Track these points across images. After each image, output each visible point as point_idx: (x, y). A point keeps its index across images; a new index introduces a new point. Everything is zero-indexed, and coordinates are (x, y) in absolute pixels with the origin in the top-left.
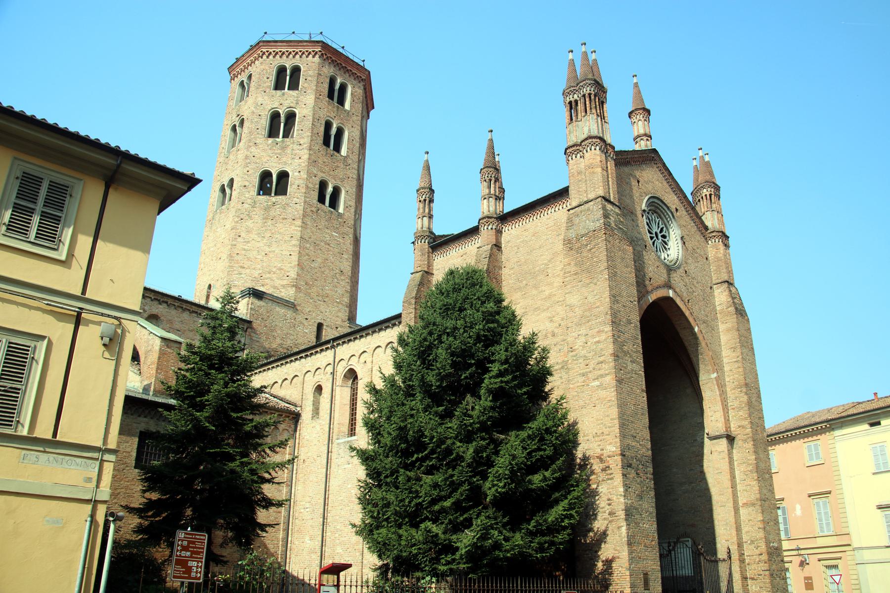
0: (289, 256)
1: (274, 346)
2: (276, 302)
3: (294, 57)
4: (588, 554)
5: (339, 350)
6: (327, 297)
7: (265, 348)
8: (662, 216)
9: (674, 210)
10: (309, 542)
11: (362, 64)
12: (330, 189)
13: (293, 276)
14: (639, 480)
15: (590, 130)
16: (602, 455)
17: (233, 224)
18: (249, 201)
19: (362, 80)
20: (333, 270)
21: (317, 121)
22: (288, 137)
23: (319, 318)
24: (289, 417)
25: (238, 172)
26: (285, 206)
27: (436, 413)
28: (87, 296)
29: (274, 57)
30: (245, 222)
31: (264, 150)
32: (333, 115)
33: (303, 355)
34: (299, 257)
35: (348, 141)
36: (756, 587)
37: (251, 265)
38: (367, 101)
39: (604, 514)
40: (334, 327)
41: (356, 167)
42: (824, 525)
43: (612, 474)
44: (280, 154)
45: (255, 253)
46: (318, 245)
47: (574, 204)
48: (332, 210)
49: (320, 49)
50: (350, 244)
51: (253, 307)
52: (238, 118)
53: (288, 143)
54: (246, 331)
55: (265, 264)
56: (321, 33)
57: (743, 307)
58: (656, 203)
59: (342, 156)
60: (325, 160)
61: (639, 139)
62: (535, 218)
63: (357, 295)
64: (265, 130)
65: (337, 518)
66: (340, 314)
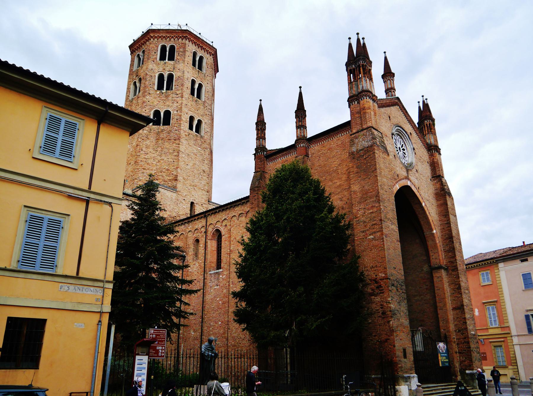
4: (370, 338)
6: (196, 186)
8: (403, 137)
9: (409, 134)
10: (193, 333)
11: (211, 44)
14: (398, 293)
15: (363, 87)
16: (376, 279)
19: (212, 54)
21: (186, 80)
24: (179, 258)
26: (169, 132)
28: (92, 190)
31: (155, 98)
32: (195, 76)
35: (205, 92)
36: (463, 358)
39: (379, 314)
40: (200, 204)
42: (493, 321)
43: (383, 290)
47: (354, 131)
52: (137, 77)
53: (169, 94)
56: (187, 25)
57: (450, 191)
58: (399, 130)
61: (388, 91)
62: (329, 140)
65: (211, 318)
66: (203, 197)
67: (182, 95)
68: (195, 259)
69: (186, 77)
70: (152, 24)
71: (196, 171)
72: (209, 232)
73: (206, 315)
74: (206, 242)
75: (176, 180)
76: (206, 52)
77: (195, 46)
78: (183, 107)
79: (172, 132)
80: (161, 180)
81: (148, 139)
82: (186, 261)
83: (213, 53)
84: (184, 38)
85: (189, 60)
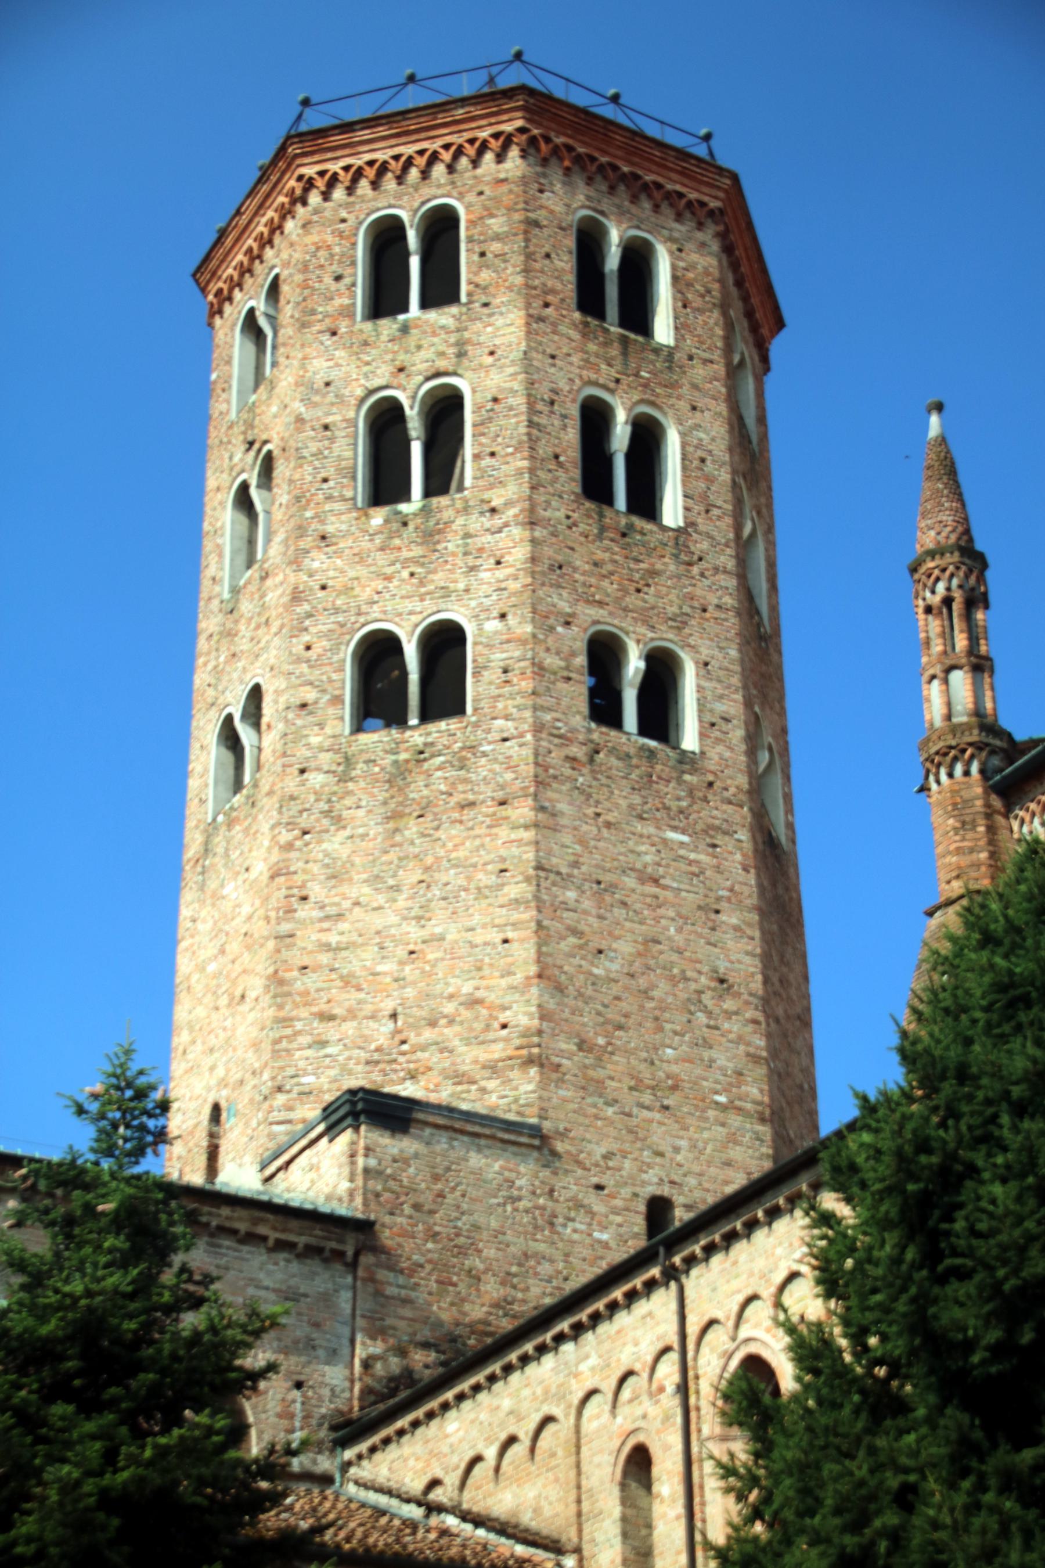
0: (500, 947)
1: (476, 1312)
2: (462, 1132)
3: (425, 174)
5: (697, 1280)
6: (675, 1088)
7: (439, 1324)
11: (701, 151)
12: (634, 665)
13: (524, 1021)
17: (275, 856)
18: (325, 758)
19: (711, 213)
20: (687, 979)
21: (546, 409)
25: (271, 656)
27: (1009, 1482)
29: (350, 190)
30: (320, 842)
31: (360, 558)
32: (606, 373)
33: (564, 1326)
34: (539, 946)
35: (684, 468)
38: (745, 298)
41: (731, 564)
45: (369, 954)
46: (612, 887)
48: (653, 743)
49: (519, 123)
50: (746, 869)
51: (372, 1162)
52: (252, 453)
53: (448, 514)
54: (353, 1266)
55: (410, 992)
59: (665, 529)
60: (600, 555)
63: (809, 1072)
64: (354, 478)
66: (736, 1153)
77: (590, 181)
79: (484, 754)
81: (338, 821)
83: (714, 204)
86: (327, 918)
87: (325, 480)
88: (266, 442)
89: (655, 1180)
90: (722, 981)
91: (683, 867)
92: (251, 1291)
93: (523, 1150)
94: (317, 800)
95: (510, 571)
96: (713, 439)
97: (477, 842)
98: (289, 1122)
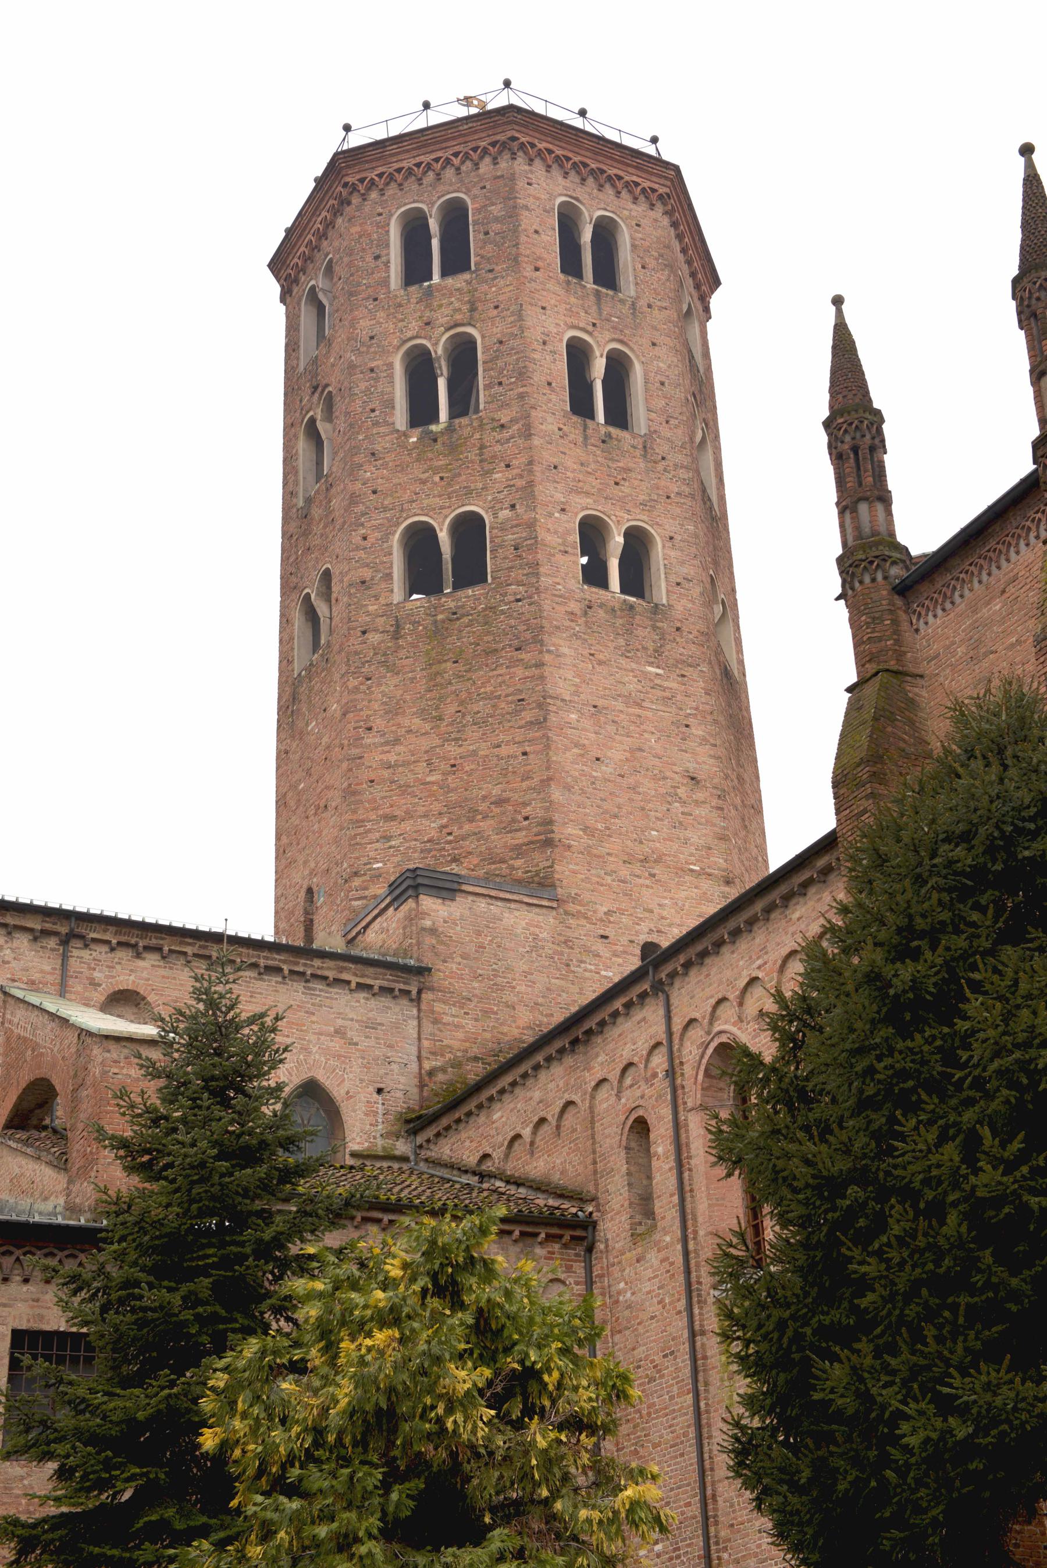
0: (521, 758)
2: (497, 898)
11: (650, 150)
19: (661, 197)
22: (464, 413)
23: (644, 927)
24: (561, 1237)
31: (401, 468)
32: (584, 320)
35: (647, 390)
37: (415, 805)
44: (445, 468)
48: (633, 599)
52: (317, 395)
54: (419, 999)
67: (528, 427)
68: (640, 1229)
69: (534, 334)
70: (347, 128)
71: (647, 786)
72: (688, 1070)
73: (725, 1549)
74: (677, 1126)
75: (549, 843)
76: (624, 194)
77: (566, 175)
78: (538, 476)
79: (503, 612)
80: (475, 860)
82: (602, 1246)
83: (662, 190)
84: (500, 152)
85: (539, 251)
86: (387, 743)
87: (373, 411)
88: (327, 385)
89: (646, 930)
90: (693, 779)
91: (660, 693)
92: (340, 1022)
93: (544, 911)
94: (376, 654)
95: (516, 471)
96: (669, 367)
97: (500, 679)
98: (365, 898)
